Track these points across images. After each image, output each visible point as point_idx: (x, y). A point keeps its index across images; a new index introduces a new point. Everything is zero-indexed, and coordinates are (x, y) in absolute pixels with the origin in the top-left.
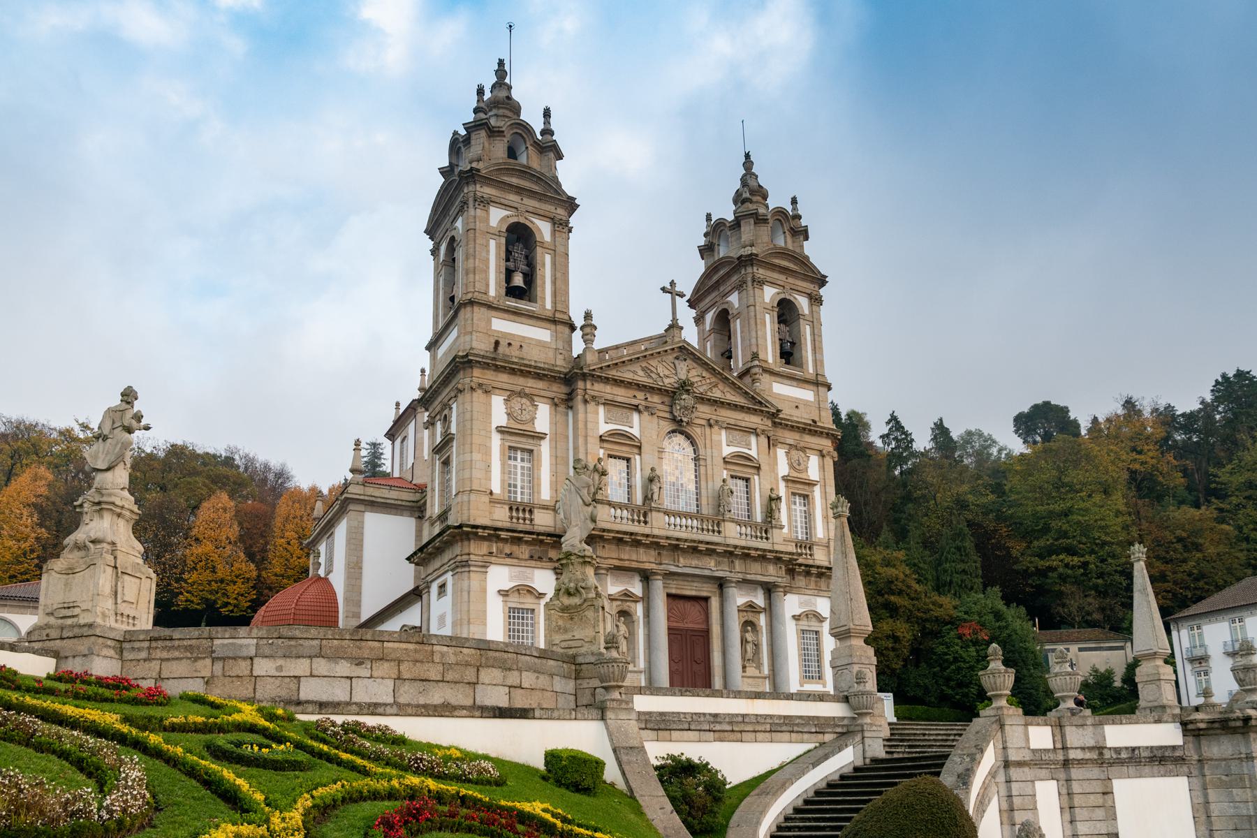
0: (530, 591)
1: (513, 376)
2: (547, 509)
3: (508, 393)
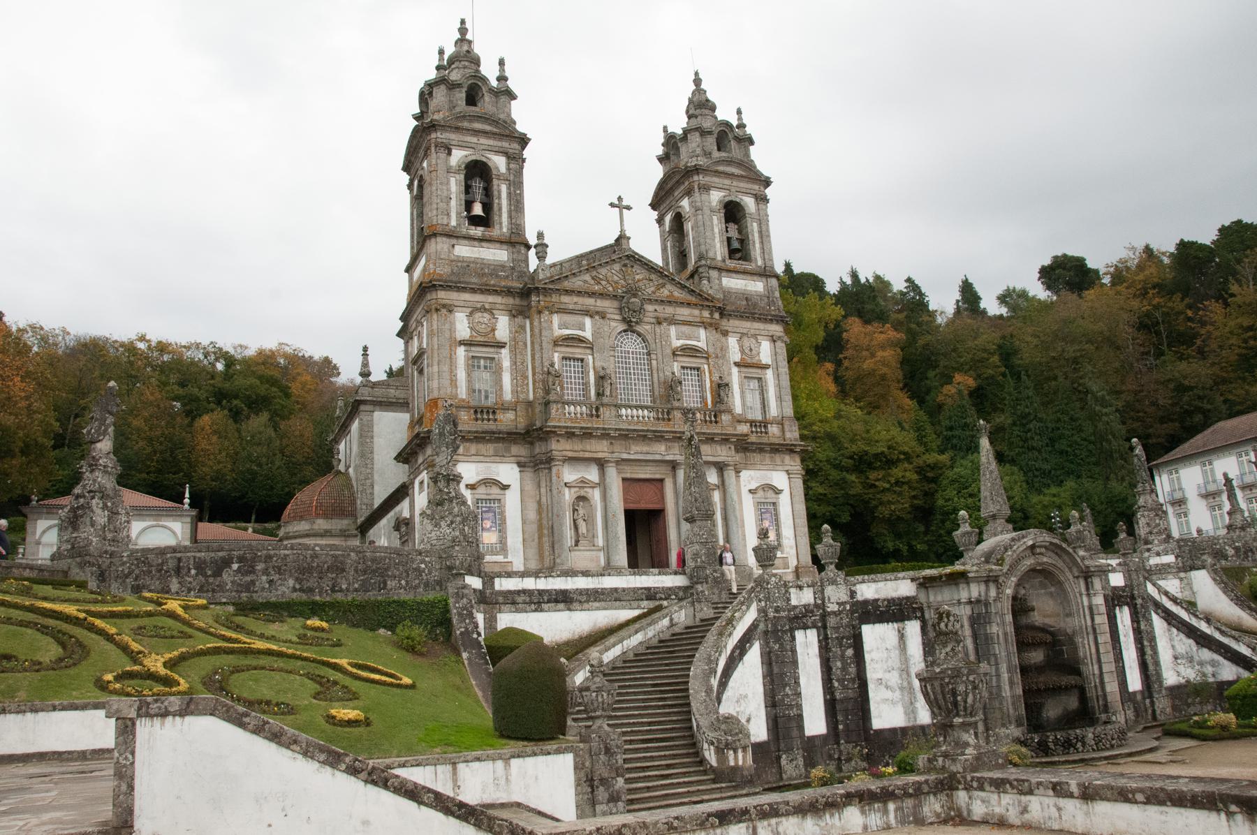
0: (495, 483)
1: (473, 295)
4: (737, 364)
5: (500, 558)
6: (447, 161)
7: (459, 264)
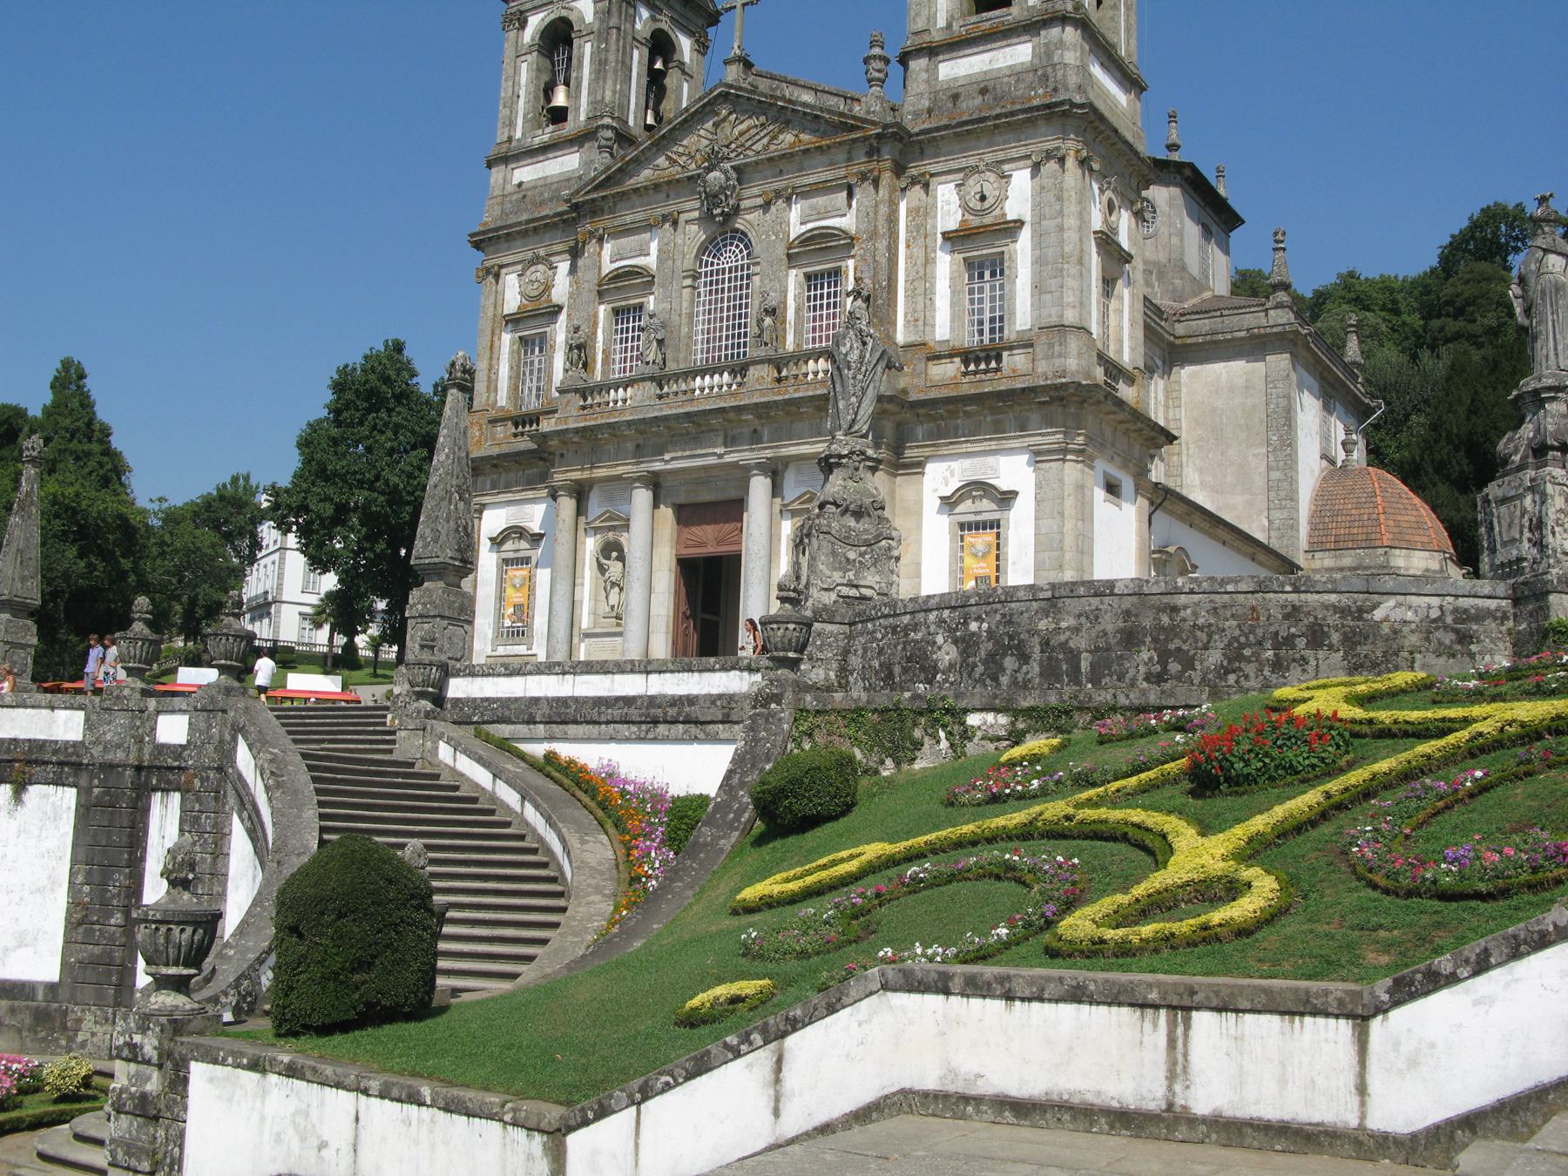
4: (947, 236)
5: (522, 649)
7: (514, 197)
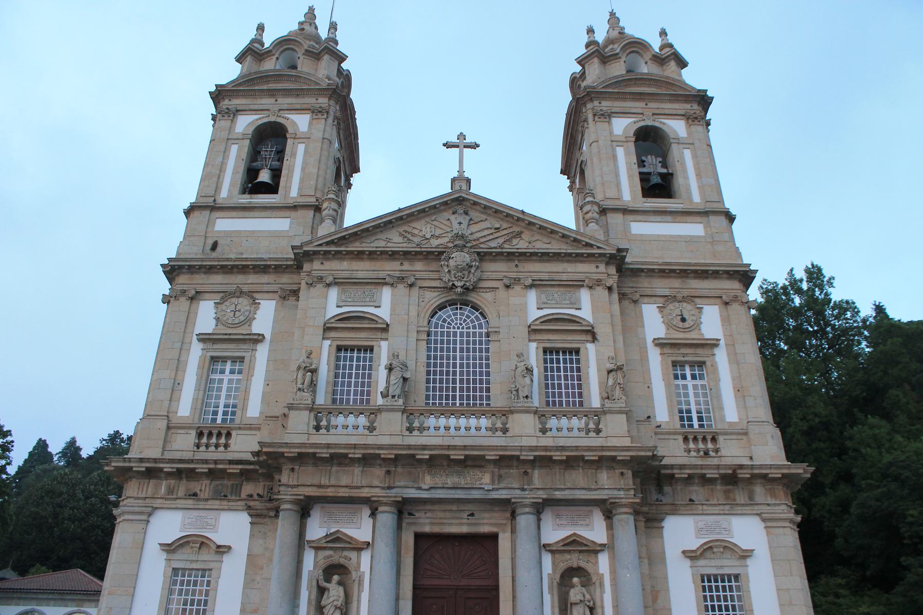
0: (203, 543)
2: (250, 429)
3: (222, 295)
6: (231, 129)
